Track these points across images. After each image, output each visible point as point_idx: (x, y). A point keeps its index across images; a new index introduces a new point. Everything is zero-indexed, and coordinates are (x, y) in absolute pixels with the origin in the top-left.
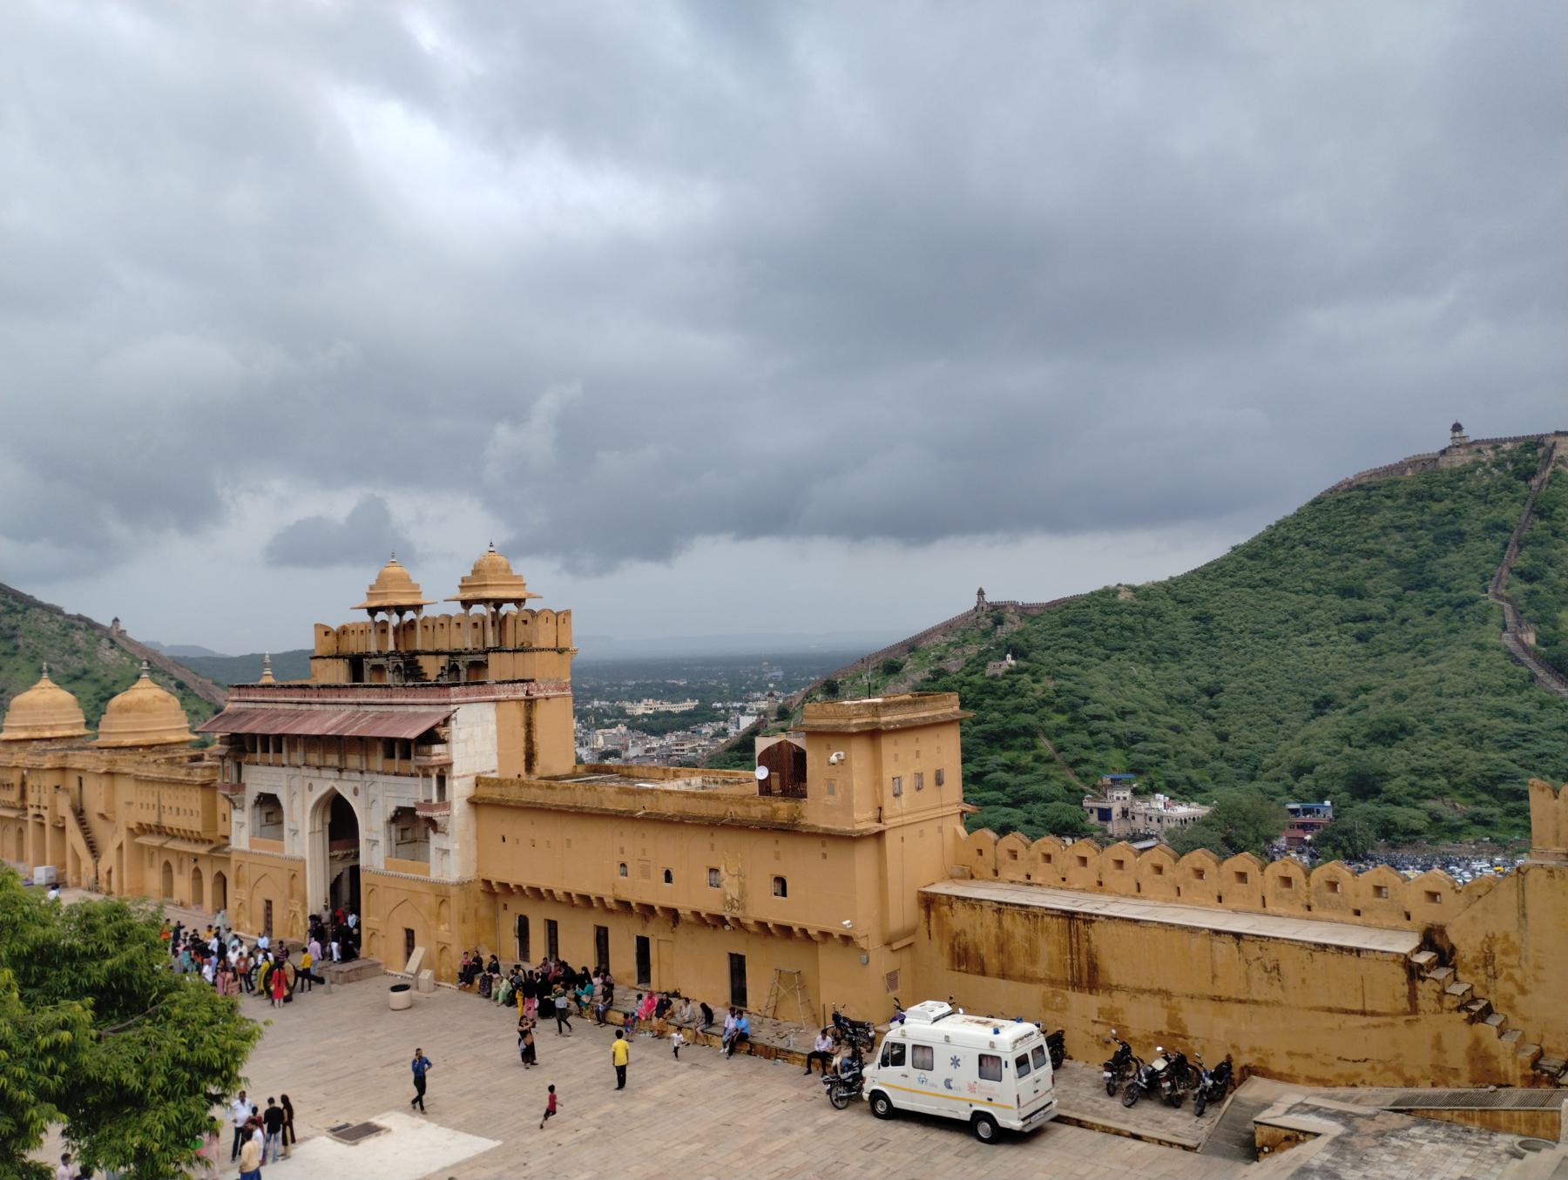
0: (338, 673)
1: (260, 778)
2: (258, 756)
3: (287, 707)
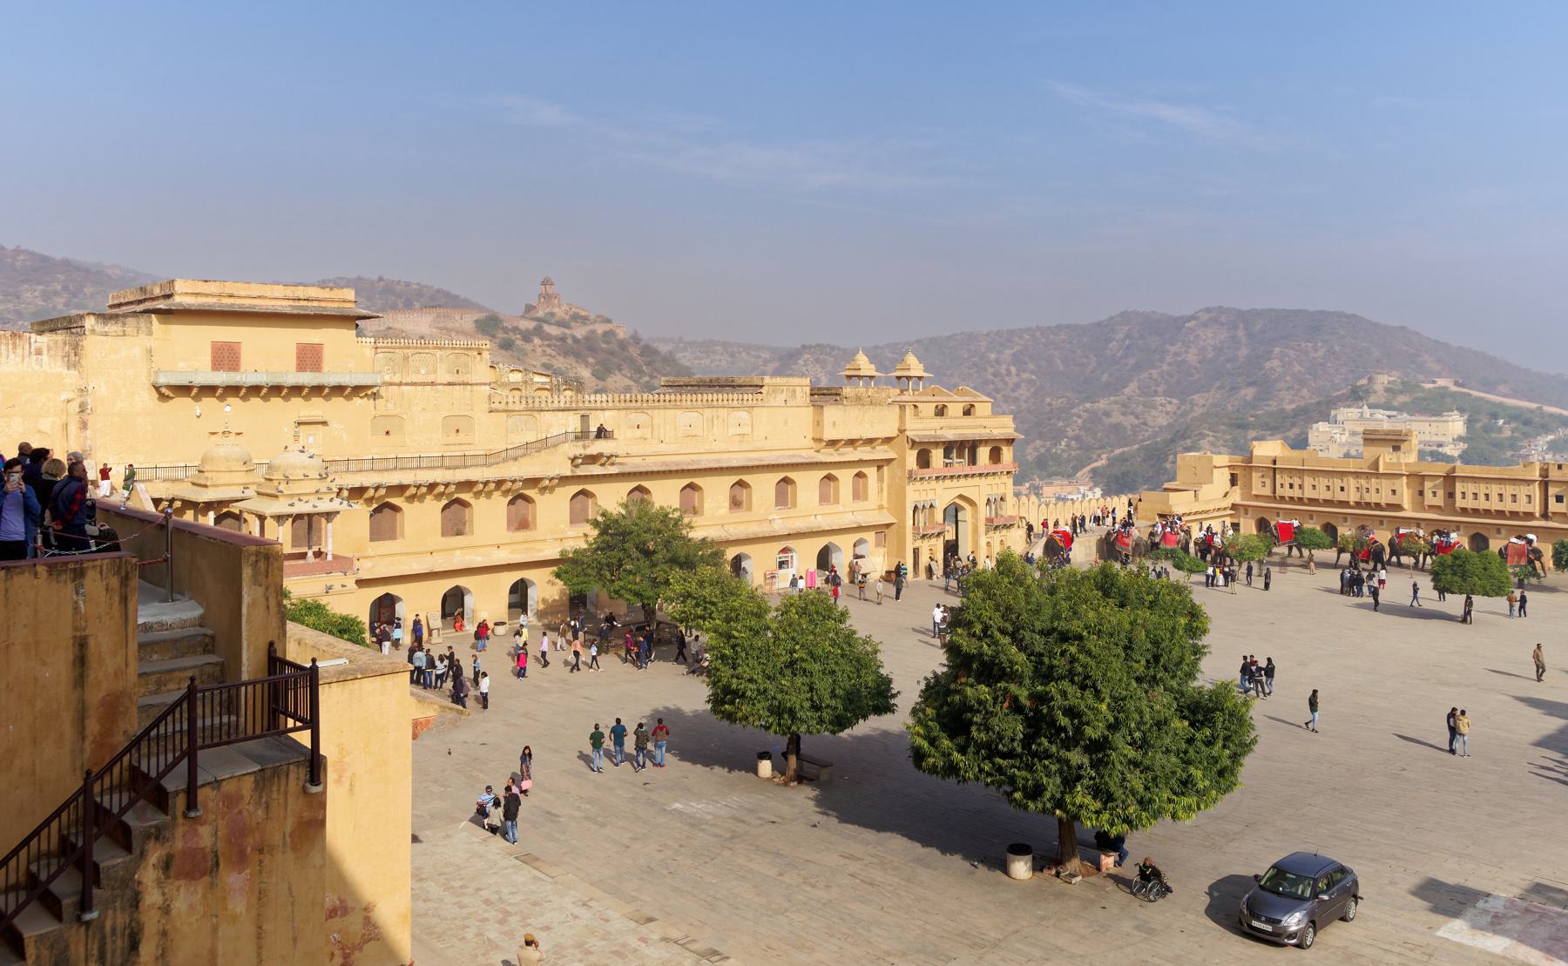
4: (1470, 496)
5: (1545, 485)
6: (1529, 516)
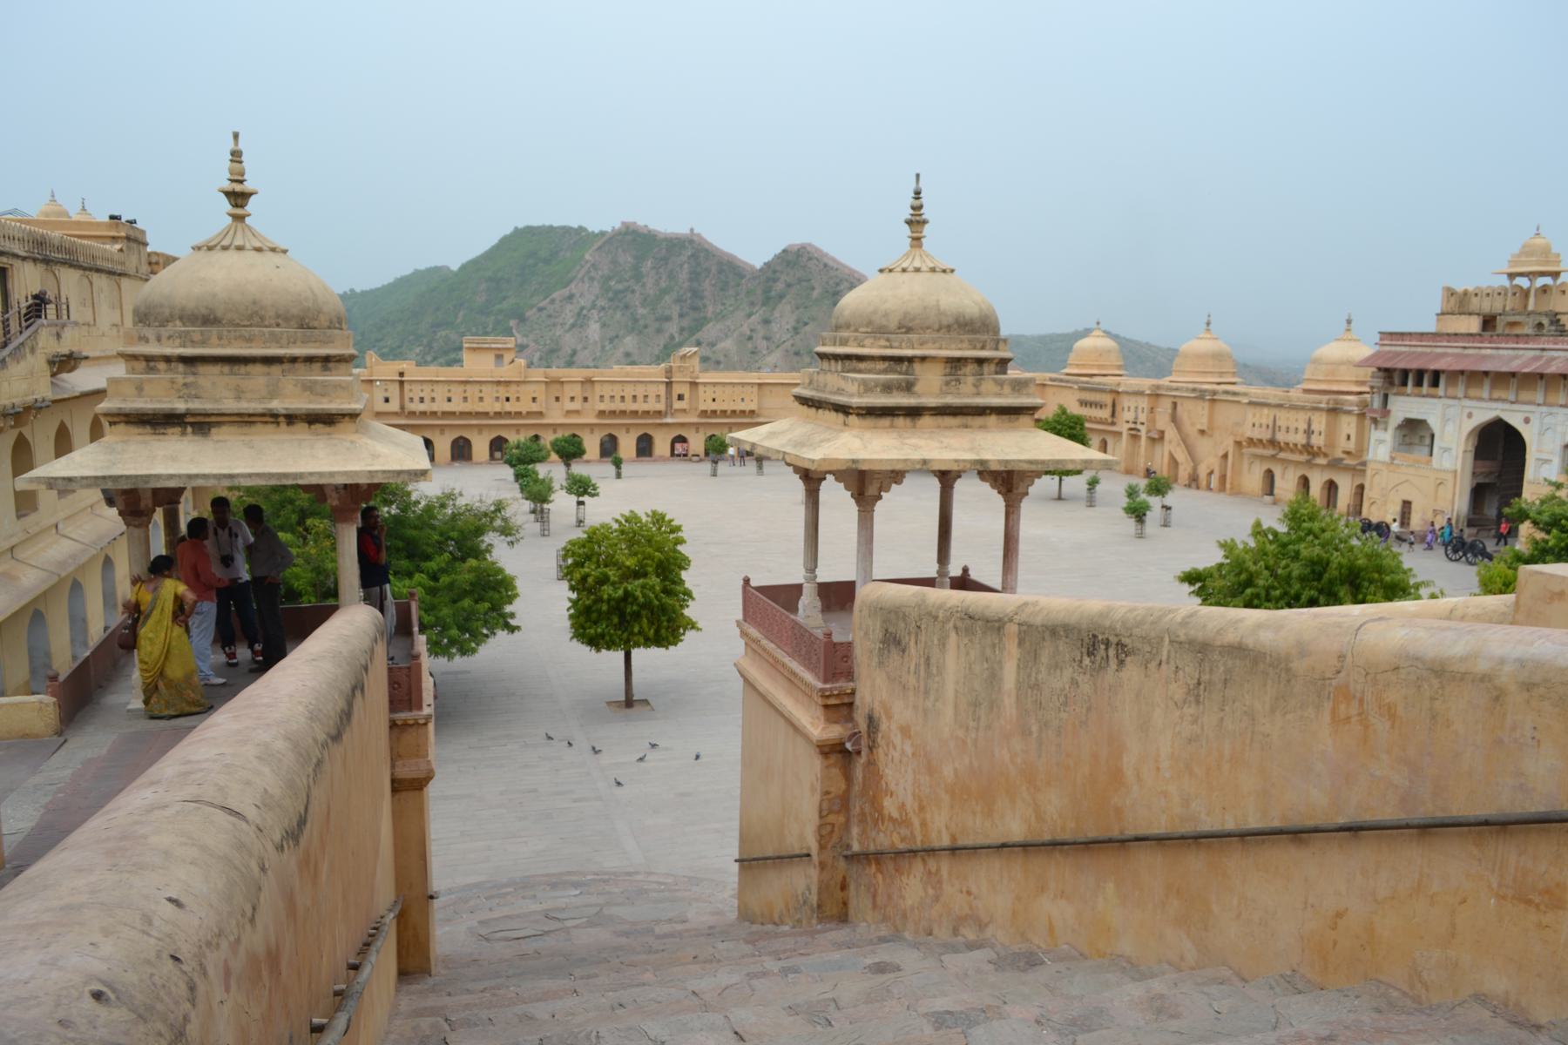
0: (1473, 325)
1: (1405, 406)
2: (1410, 388)
3: (1450, 351)
4: (607, 399)
5: (669, 384)
6: (659, 413)
